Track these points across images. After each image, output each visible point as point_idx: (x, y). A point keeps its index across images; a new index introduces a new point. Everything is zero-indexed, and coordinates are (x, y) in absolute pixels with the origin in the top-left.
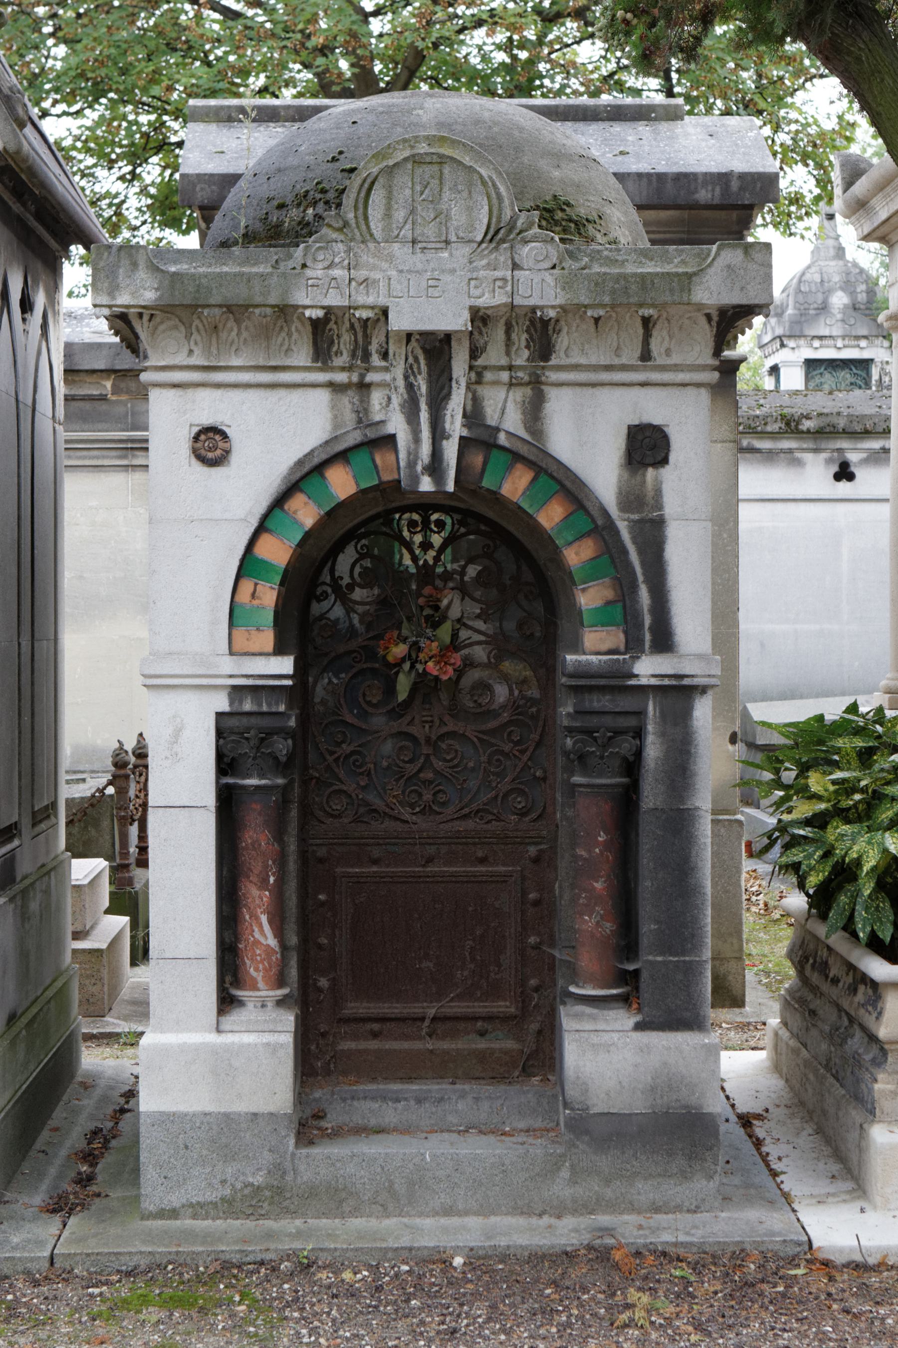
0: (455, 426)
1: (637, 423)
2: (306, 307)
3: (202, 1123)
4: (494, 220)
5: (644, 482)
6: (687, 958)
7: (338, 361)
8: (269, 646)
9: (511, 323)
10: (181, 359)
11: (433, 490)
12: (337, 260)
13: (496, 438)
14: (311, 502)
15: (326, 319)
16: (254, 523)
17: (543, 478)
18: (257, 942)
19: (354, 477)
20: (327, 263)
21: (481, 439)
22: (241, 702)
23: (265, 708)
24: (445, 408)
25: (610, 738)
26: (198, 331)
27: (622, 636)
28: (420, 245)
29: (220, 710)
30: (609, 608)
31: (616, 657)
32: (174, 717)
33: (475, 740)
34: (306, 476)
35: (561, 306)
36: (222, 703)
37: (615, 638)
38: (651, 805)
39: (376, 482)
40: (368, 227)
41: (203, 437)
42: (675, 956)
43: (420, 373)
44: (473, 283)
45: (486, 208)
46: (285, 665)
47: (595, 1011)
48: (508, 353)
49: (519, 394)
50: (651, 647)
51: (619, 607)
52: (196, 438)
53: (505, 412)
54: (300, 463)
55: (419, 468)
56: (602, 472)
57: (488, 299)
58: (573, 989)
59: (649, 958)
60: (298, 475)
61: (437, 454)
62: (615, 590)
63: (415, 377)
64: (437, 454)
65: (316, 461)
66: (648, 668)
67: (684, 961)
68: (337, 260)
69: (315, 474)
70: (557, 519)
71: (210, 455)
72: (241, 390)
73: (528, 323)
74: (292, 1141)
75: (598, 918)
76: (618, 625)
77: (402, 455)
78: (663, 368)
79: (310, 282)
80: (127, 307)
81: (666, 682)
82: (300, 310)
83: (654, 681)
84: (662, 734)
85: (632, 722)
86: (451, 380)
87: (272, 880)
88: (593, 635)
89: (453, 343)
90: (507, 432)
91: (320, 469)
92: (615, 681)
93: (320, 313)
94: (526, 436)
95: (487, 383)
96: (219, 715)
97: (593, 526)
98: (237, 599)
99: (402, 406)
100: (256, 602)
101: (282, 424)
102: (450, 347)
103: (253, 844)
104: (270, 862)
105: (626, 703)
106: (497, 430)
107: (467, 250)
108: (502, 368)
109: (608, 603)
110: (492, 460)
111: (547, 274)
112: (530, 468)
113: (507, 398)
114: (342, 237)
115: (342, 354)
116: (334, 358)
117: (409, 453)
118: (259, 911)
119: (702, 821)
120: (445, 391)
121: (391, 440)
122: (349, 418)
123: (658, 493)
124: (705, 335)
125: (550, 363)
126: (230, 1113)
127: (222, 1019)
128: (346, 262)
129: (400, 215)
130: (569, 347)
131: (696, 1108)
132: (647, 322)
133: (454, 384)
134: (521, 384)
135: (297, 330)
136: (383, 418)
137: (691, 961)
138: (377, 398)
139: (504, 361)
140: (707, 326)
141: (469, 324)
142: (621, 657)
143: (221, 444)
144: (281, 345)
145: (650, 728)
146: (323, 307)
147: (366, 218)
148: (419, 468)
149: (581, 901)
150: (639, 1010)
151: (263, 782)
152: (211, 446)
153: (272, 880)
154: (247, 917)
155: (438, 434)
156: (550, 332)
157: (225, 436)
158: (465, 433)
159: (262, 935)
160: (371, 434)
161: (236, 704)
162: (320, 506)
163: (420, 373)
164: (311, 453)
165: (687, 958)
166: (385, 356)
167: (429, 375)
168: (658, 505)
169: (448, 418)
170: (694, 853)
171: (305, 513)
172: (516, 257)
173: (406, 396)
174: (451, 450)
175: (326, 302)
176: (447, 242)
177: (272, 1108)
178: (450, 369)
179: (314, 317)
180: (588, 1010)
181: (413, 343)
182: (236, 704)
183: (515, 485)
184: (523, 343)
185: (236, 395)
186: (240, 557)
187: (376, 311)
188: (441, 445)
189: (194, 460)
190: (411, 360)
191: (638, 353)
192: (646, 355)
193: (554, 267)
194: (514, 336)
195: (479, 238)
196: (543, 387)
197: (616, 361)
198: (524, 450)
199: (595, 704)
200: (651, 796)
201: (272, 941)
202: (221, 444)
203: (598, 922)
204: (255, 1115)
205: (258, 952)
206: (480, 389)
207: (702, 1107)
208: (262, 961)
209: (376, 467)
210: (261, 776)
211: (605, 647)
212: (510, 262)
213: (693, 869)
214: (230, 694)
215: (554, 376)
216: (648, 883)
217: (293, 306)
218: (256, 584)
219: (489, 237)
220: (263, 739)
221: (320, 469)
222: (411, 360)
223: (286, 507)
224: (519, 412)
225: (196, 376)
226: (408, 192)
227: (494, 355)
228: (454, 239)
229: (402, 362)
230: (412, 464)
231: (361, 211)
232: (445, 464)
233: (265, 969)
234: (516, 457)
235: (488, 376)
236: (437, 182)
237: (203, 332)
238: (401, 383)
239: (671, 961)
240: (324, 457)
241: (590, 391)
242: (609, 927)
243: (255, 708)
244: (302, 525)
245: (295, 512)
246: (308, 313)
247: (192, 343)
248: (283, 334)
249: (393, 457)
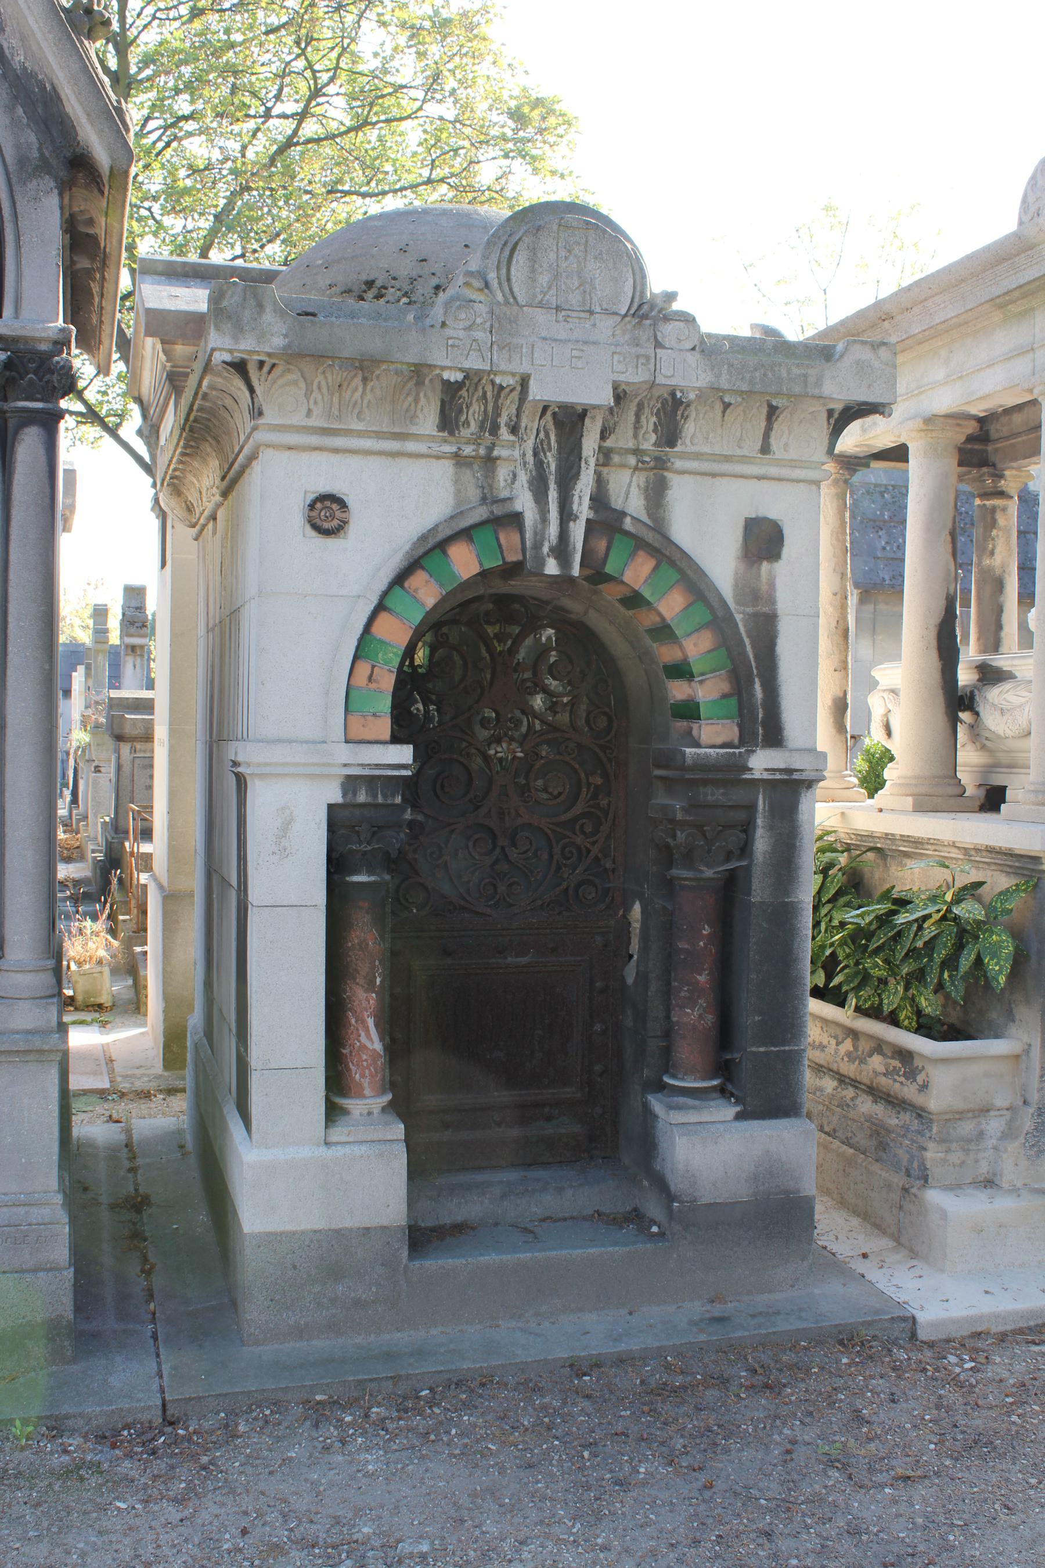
0: (583, 508)
1: (754, 516)
2: (443, 368)
3: (312, 1241)
4: (638, 294)
5: (759, 575)
6: (787, 1048)
7: (465, 433)
8: (387, 735)
9: (643, 404)
10: (298, 419)
11: (558, 573)
12: (479, 321)
13: (622, 522)
14: (432, 580)
15: (459, 385)
16: (374, 601)
17: (665, 566)
18: (363, 1047)
19: (478, 556)
20: (468, 323)
21: (606, 521)
22: (355, 794)
23: (380, 800)
24: (573, 488)
25: (721, 831)
26: (319, 388)
27: (736, 729)
28: (563, 313)
29: (332, 802)
30: (724, 701)
31: (732, 750)
32: (283, 808)
33: (549, 832)
34: (427, 554)
35: (699, 389)
36: (336, 796)
37: (729, 731)
38: (758, 899)
39: (501, 563)
40: (511, 289)
41: (319, 505)
42: (776, 1046)
43: (550, 450)
44: (616, 357)
45: (631, 281)
46: (404, 754)
47: (697, 1103)
48: (635, 436)
49: (640, 478)
50: (762, 741)
51: (734, 701)
52: (312, 506)
53: (628, 494)
54: (423, 538)
55: (546, 549)
56: (721, 563)
57: (634, 376)
58: (667, 1079)
59: (752, 1049)
60: (422, 551)
61: (564, 535)
62: (731, 682)
63: (545, 454)
64: (564, 535)
65: (441, 536)
66: (762, 762)
67: (784, 1051)
68: (479, 321)
69: (437, 551)
70: (677, 609)
71: (326, 525)
72: (361, 457)
73: (659, 405)
74: (405, 1253)
75: (701, 1011)
76: (731, 718)
77: (529, 535)
78: (779, 463)
79: (450, 342)
80: (250, 352)
81: (778, 776)
82: (438, 371)
83: (766, 776)
84: (771, 828)
85: (742, 816)
86: (580, 459)
87: (378, 980)
88: (709, 728)
89: (587, 421)
90: (633, 518)
91: (442, 546)
92: (730, 772)
93: (459, 376)
94: (649, 522)
95: (615, 466)
96: (330, 807)
97: (710, 617)
98: (352, 682)
99: (530, 483)
100: (373, 686)
101: (403, 495)
102: (583, 425)
103: (360, 944)
104: (377, 963)
105: (738, 796)
106: (624, 514)
107: (612, 321)
108: (628, 451)
109: (725, 696)
110: (616, 543)
111: (688, 354)
112: (652, 556)
113: (631, 482)
114: (482, 298)
115: (469, 425)
116: (461, 429)
117: (535, 533)
118: (366, 1014)
119: (805, 913)
120: (574, 471)
121: (516, 519)
122: (473, 494)
123: (772, 586)
124: (822, 430)
125: (675, 449)
126: (340, 1229)
127: (331, 1131)
128: (488, 324)
129: (544, 279)
130: (697, 432)
131: (794, 1193)
132: (772, 412)
133: (583, 464)
134: (645, 469)
135: (425, 395)
136: (508, 496)
137: (790, 1051)
138: (502, 473)
139: (631, 444)
140: (825, 423)
141: (612, 400)
142: (737, 751)
143: (338, 514)
144: (407, 411)
145: (760, 822)
146: (461, 370)
147: (509, 280)
148: (546, 549)
149: (682, 994)
150: (738, 1102)
151: (372, 878)
152: (327, 515)
153: (378, 980)
154: (353, 1021)
155: (566, 515)
156: (679, 417)
157: (342, 504)
158: (591, 516)
159: (368, 1039)
160: (498, 510)
161: (350, 795)
162: (441, 585)
163: (550, 450)
164: (434, 529)
165: (787, 1048)
166: (514, 430)
167: (559, 452)
168: (772, 600)
169: (576, 499)
170: (796, 946)
171: (427, 593)
172: (659, 334)
173: (534, 473)
174: (578, 532)
175: (467, 365)
176: (591, 313)
177: (385, 1222)
178: (581, 448)
179: (452, 380)
180: (690, 1102)
181: (549, 416)
182: (350, 795)
183: (637, 572)
184: (651, 427)
185: (354, 461)
186: (358, 636)
187: (518, 378)
188: (568, 527)
189: (308, 528)
190: (542, 435)
191: (758, 445)
192: (765, 449)
193: (693, 349)
194: (643, 419)
195: (623, 312)
196: (666, 474)
197: (739, 452)
198: (649, 536)
199: (709, 798)
200: (759, 891)
201: (378, 1046)
202: (338, 514)
203: (700, 1016)
204: (368, 1229)
205: (364, 1057)
206: (605, 470)
207: (799, 1191)
208: (368, 1068)
209: (500, 546)
210: (370, 873)
211: (719, 741)
212: (652, 339)
213: (795, 961)
214: (343, 785)
215: (679, 464)
216: (753, 976)
217: (430, 366)
218: (373, 667)
219: (632, 312)
220: (374, 833)
221: (442, 546)
222: (542, 435)
223: (406, 585)
224: (642, 497)
225: (315, 440)
226: (552, 256)
227: (622, 439)
228: (598, 309)
229: (533, 437)
230: (537, 546)
231: (504, 271)
232: (571, 547)
233: (371, 1075)
234: (640, 544)
235: (616, 459)
236: (582, 248)
237: (325, 390)
238: (530, 458)
239: (772, 1052)
240: (449, 532)
241: (709, 480)
242: (710, 1019)
243: (370, 800)
244: (423, 605)
245: (416, 591)
246: (446, 375)
247: (312, 401)
248: (410, 399)
249: (516, 538)
